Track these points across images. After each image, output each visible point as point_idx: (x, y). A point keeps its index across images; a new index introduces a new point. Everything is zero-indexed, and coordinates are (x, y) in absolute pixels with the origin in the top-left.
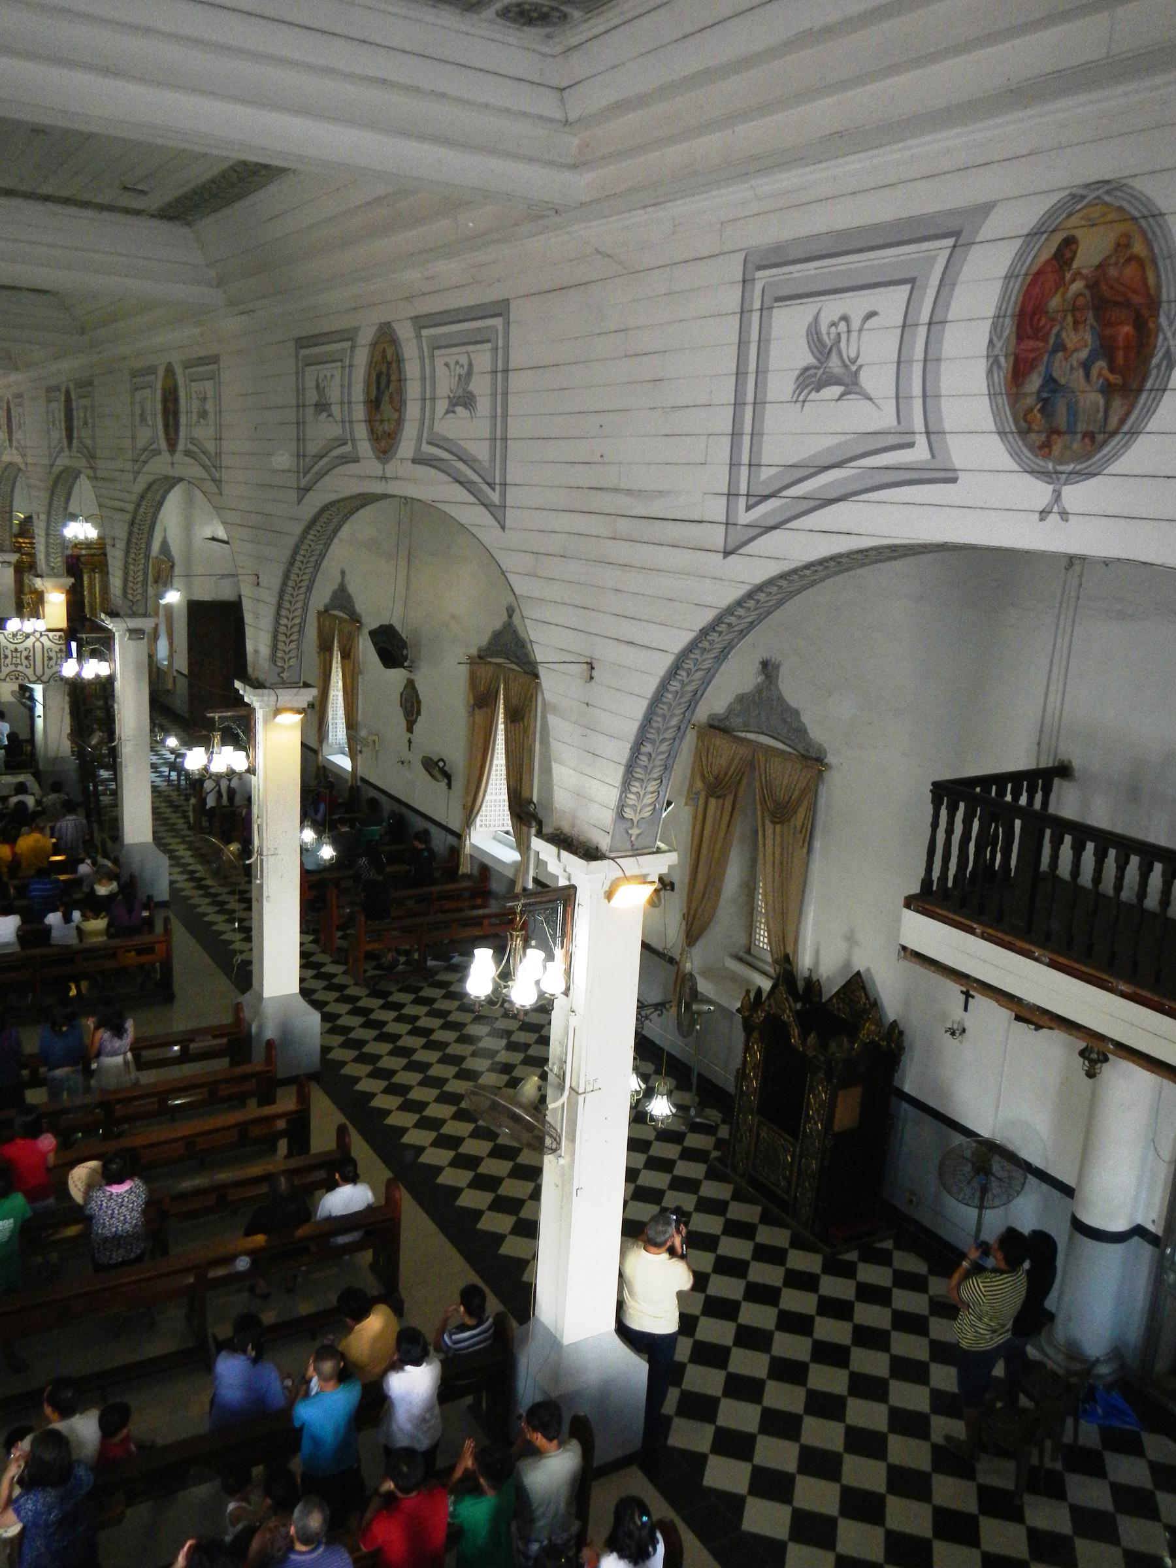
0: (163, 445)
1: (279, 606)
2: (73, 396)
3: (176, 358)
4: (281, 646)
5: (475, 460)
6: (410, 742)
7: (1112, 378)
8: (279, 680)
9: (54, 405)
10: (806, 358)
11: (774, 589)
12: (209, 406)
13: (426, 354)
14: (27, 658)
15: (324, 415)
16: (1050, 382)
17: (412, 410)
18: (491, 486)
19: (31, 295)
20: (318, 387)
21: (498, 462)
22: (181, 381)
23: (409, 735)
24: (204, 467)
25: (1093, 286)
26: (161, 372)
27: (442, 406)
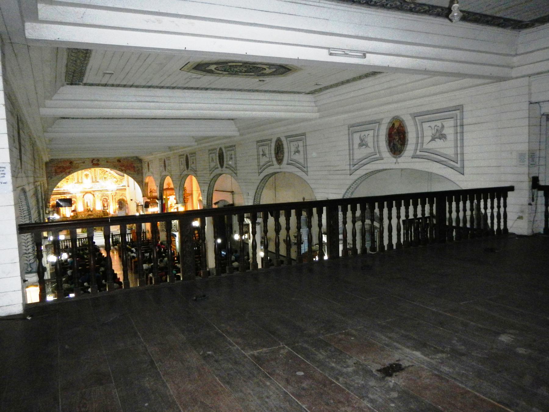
0: (219, 166)
1: (254, 199)
3: (223, 146)
7: (402, 143)
10: (359, 142)
11: (359, 180)
12: (233, 156)
14: (175, 225)
15: (265, 156)
16: (394, 144)
17: (286, 155)
18: (304, 167)
24: (232, 171)
25: (397, 130)
26: (218, 150)
27: (293, 153)
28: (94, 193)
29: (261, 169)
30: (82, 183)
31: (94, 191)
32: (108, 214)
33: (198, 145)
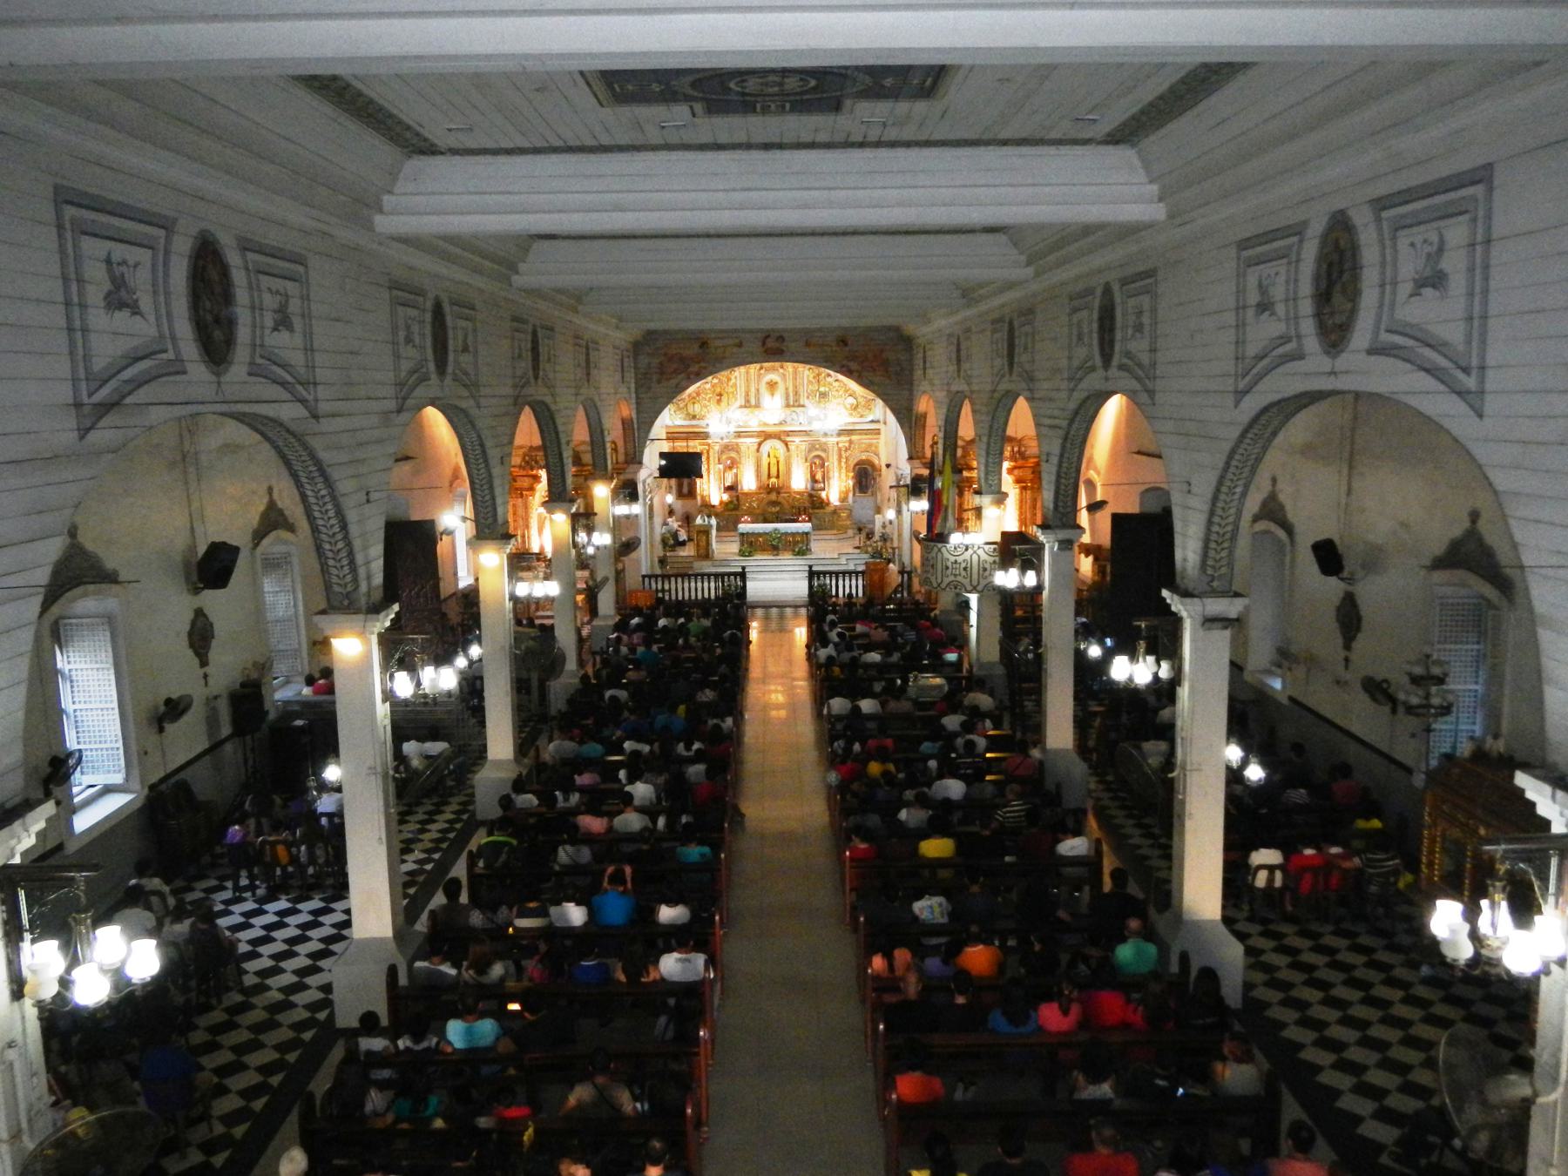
0: (1098, 361)
1: (1212, 513)
2: (1016, 324)
3: (1112, 276)
4: (1212, 553)
5: (1445, 344)
6: (1347, 660)
8: (1209, 589)
9: (998, 335)
12: (1146, 320)
13: (1386, 236)
14: (965, 569)
15: (1267, 313)
17: (1369, 298)
18: (1466, 370)
19: (984, 237)
20: (1260, 286)
21: (1475, 344)
22: (1118, 299)
23: (1347, 653)
24: (1138, 379)
26: (1099, 291)
27: (1405, 289)
28: (788, 439)
29: (1250, 370)
30: (757, 406)
31: (788, 433)
32: (822, 501)
33: (1037, 274)
